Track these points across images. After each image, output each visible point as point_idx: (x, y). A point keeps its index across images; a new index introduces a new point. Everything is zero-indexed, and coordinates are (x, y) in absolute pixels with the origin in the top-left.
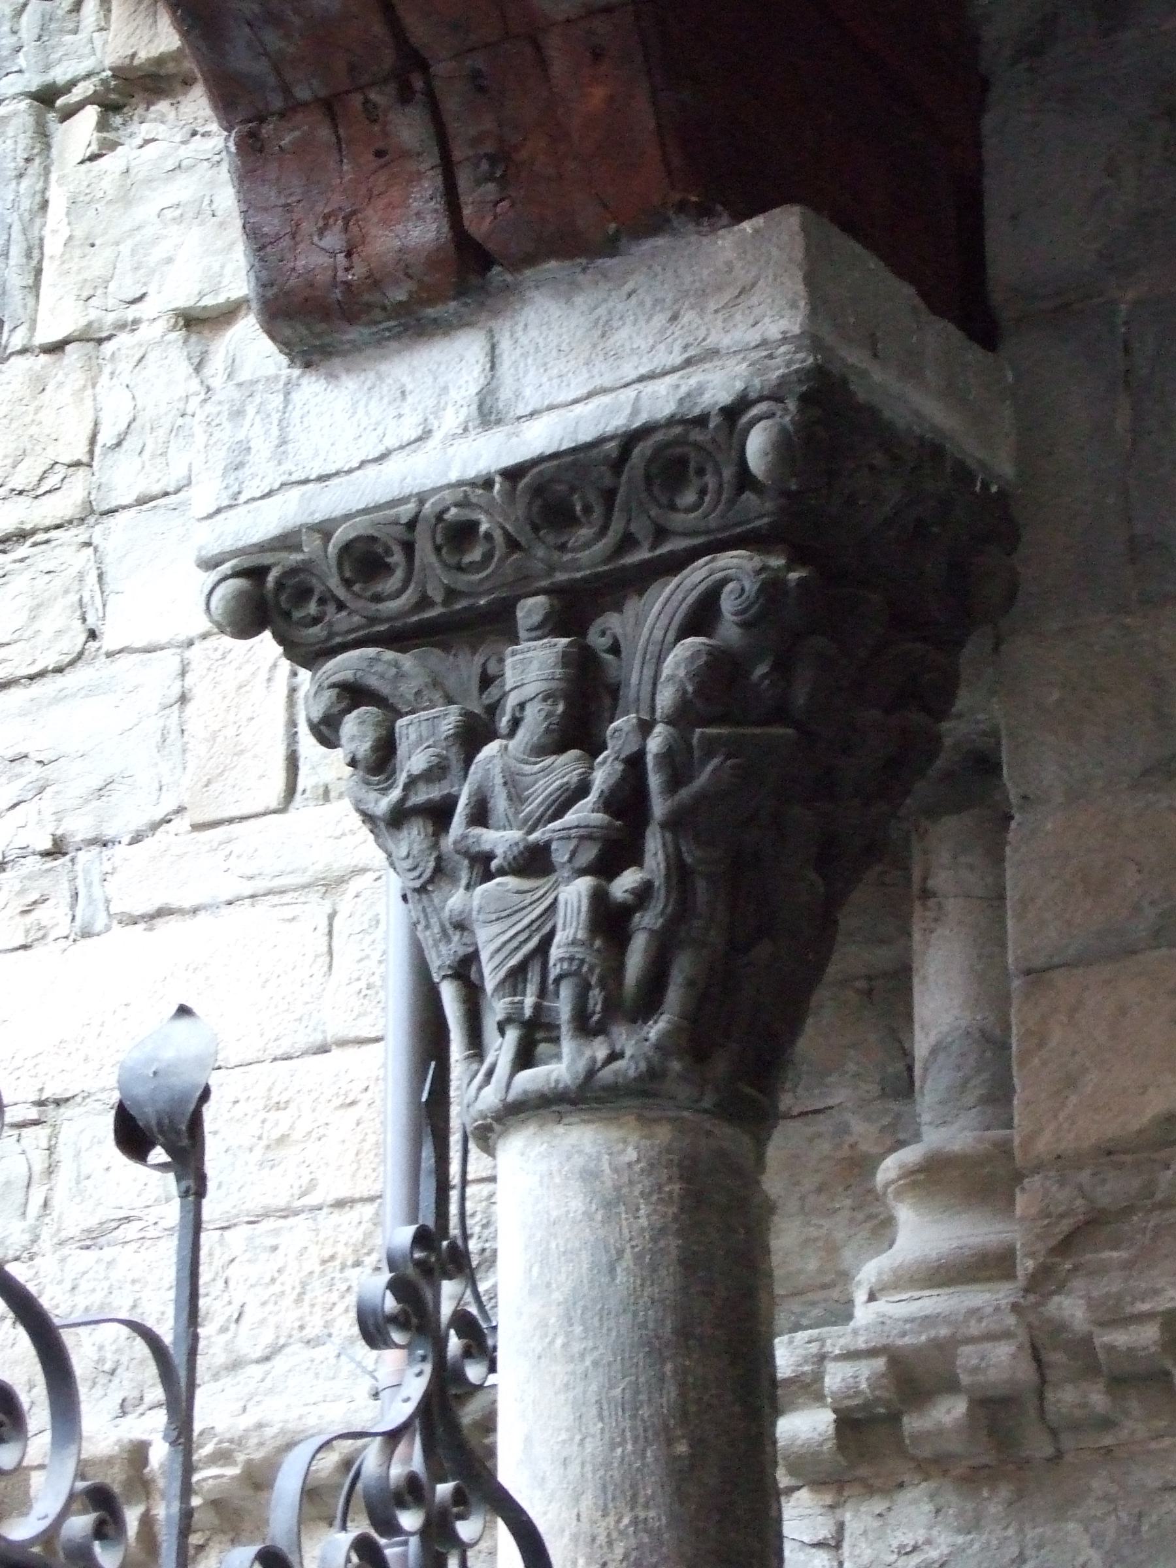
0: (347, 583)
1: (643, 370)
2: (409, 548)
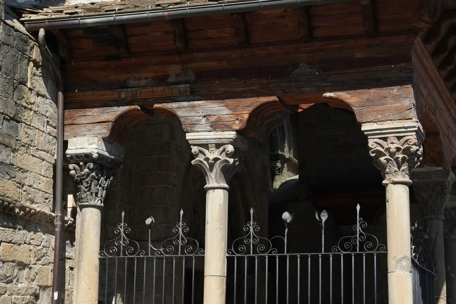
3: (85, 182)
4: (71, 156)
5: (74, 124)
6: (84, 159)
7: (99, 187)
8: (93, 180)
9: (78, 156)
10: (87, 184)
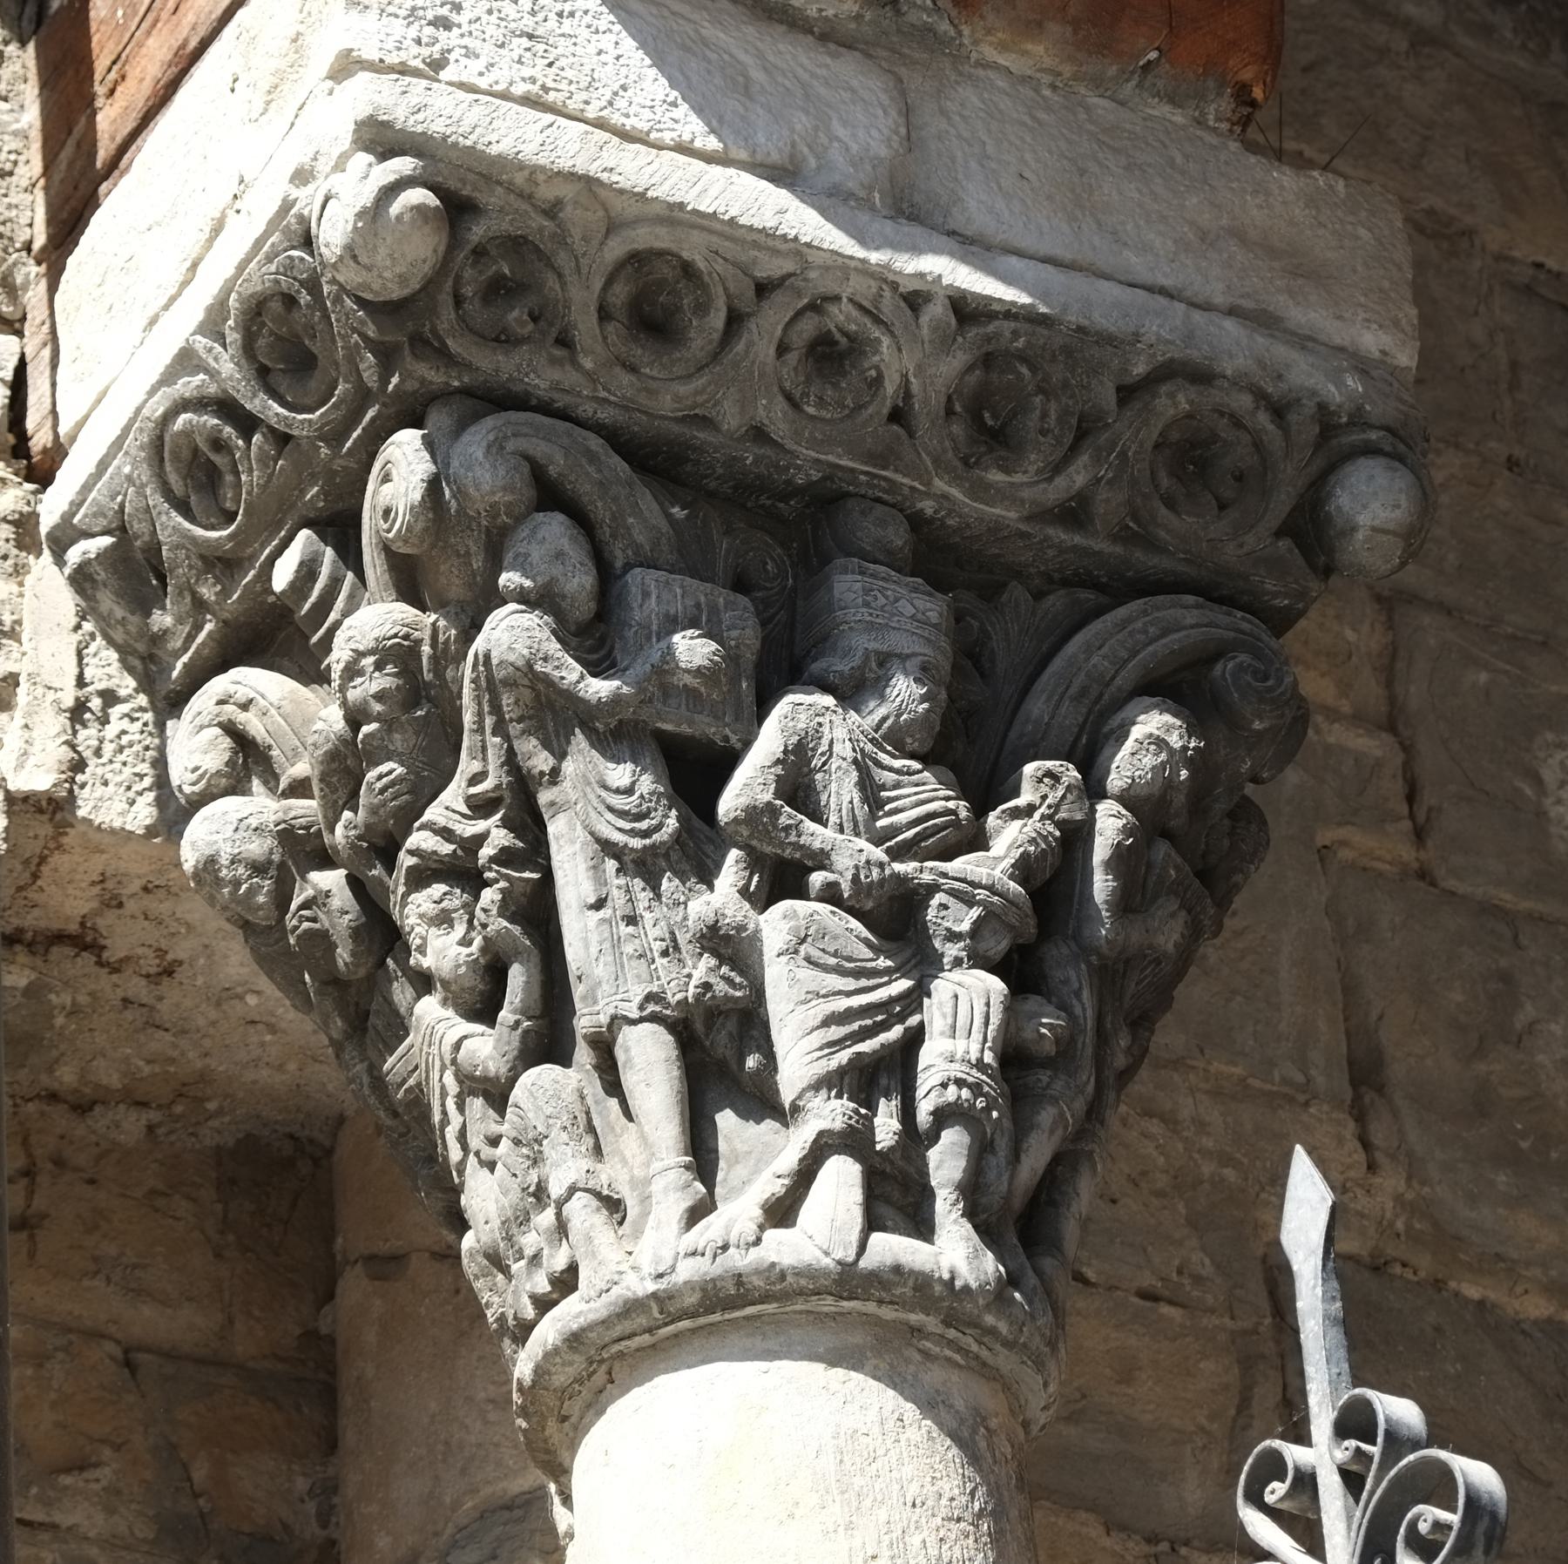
0: (604, 314)
1: (1167, 282)
2: (735, 321)
3: (426, 873)
4: (120, 529)
5: (193, 43)
6: (282, 439)
7: (763, 899)
8: (541, 761)
9: (187, 433)
10: (457, 899)
